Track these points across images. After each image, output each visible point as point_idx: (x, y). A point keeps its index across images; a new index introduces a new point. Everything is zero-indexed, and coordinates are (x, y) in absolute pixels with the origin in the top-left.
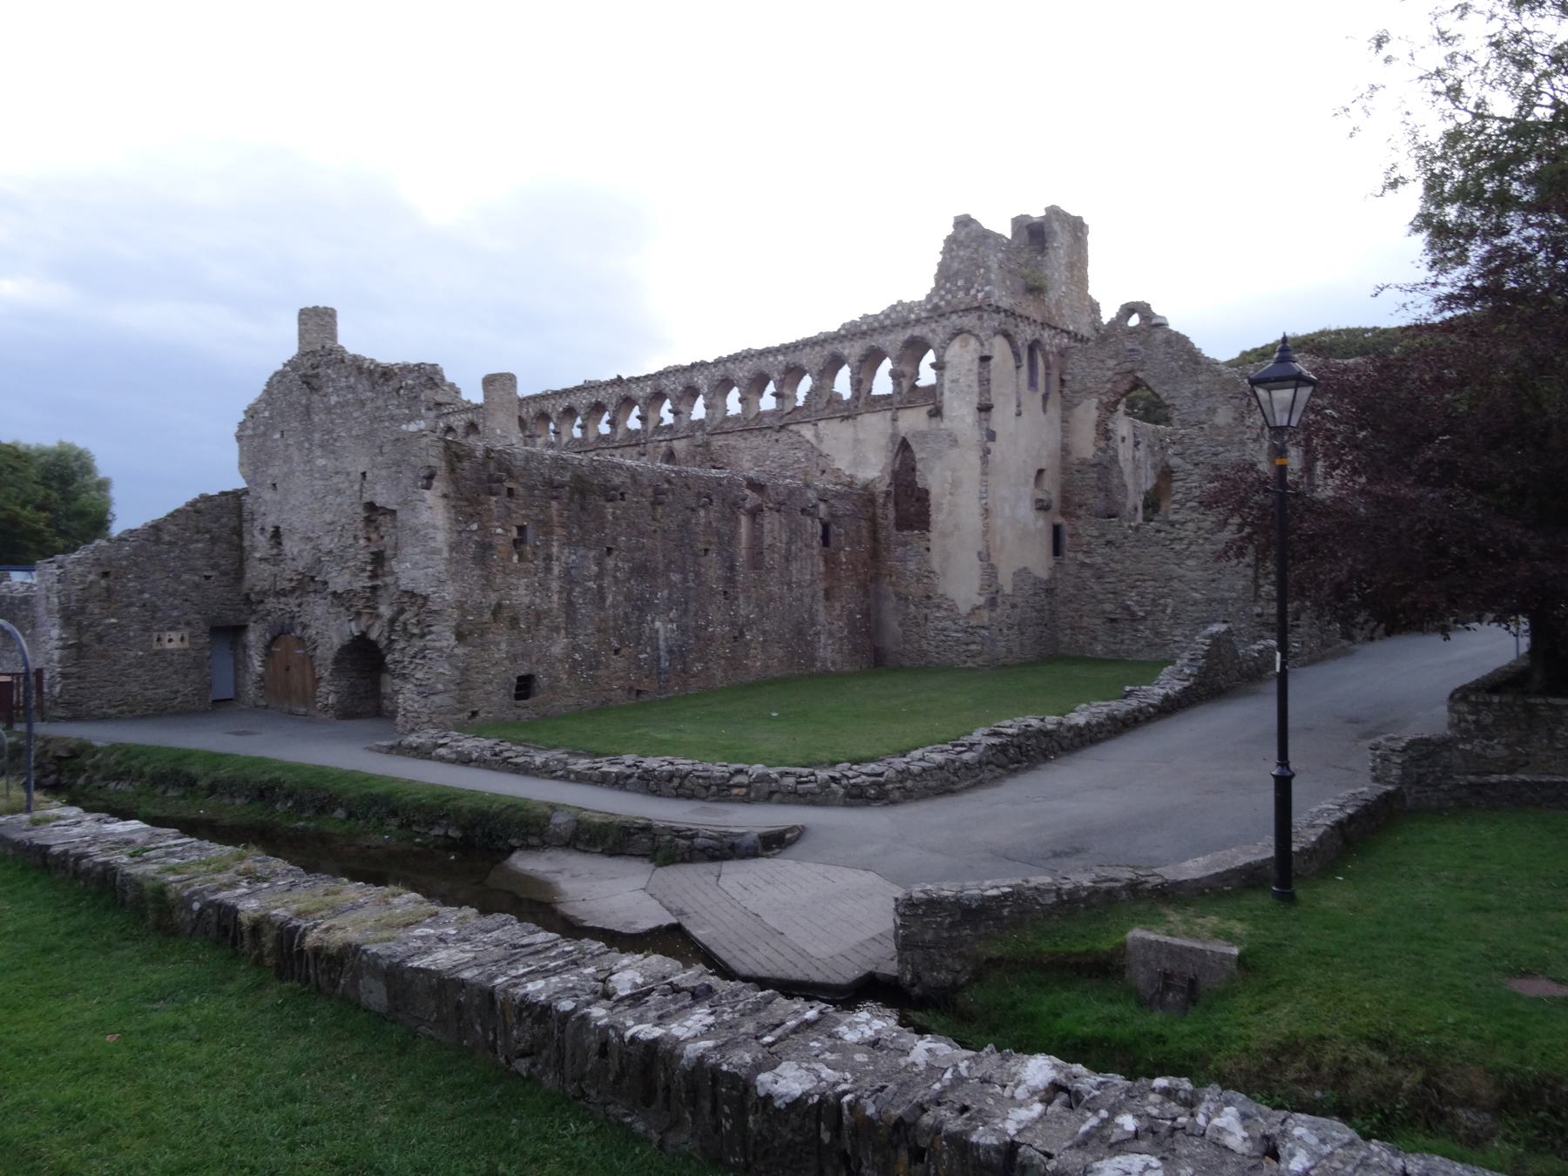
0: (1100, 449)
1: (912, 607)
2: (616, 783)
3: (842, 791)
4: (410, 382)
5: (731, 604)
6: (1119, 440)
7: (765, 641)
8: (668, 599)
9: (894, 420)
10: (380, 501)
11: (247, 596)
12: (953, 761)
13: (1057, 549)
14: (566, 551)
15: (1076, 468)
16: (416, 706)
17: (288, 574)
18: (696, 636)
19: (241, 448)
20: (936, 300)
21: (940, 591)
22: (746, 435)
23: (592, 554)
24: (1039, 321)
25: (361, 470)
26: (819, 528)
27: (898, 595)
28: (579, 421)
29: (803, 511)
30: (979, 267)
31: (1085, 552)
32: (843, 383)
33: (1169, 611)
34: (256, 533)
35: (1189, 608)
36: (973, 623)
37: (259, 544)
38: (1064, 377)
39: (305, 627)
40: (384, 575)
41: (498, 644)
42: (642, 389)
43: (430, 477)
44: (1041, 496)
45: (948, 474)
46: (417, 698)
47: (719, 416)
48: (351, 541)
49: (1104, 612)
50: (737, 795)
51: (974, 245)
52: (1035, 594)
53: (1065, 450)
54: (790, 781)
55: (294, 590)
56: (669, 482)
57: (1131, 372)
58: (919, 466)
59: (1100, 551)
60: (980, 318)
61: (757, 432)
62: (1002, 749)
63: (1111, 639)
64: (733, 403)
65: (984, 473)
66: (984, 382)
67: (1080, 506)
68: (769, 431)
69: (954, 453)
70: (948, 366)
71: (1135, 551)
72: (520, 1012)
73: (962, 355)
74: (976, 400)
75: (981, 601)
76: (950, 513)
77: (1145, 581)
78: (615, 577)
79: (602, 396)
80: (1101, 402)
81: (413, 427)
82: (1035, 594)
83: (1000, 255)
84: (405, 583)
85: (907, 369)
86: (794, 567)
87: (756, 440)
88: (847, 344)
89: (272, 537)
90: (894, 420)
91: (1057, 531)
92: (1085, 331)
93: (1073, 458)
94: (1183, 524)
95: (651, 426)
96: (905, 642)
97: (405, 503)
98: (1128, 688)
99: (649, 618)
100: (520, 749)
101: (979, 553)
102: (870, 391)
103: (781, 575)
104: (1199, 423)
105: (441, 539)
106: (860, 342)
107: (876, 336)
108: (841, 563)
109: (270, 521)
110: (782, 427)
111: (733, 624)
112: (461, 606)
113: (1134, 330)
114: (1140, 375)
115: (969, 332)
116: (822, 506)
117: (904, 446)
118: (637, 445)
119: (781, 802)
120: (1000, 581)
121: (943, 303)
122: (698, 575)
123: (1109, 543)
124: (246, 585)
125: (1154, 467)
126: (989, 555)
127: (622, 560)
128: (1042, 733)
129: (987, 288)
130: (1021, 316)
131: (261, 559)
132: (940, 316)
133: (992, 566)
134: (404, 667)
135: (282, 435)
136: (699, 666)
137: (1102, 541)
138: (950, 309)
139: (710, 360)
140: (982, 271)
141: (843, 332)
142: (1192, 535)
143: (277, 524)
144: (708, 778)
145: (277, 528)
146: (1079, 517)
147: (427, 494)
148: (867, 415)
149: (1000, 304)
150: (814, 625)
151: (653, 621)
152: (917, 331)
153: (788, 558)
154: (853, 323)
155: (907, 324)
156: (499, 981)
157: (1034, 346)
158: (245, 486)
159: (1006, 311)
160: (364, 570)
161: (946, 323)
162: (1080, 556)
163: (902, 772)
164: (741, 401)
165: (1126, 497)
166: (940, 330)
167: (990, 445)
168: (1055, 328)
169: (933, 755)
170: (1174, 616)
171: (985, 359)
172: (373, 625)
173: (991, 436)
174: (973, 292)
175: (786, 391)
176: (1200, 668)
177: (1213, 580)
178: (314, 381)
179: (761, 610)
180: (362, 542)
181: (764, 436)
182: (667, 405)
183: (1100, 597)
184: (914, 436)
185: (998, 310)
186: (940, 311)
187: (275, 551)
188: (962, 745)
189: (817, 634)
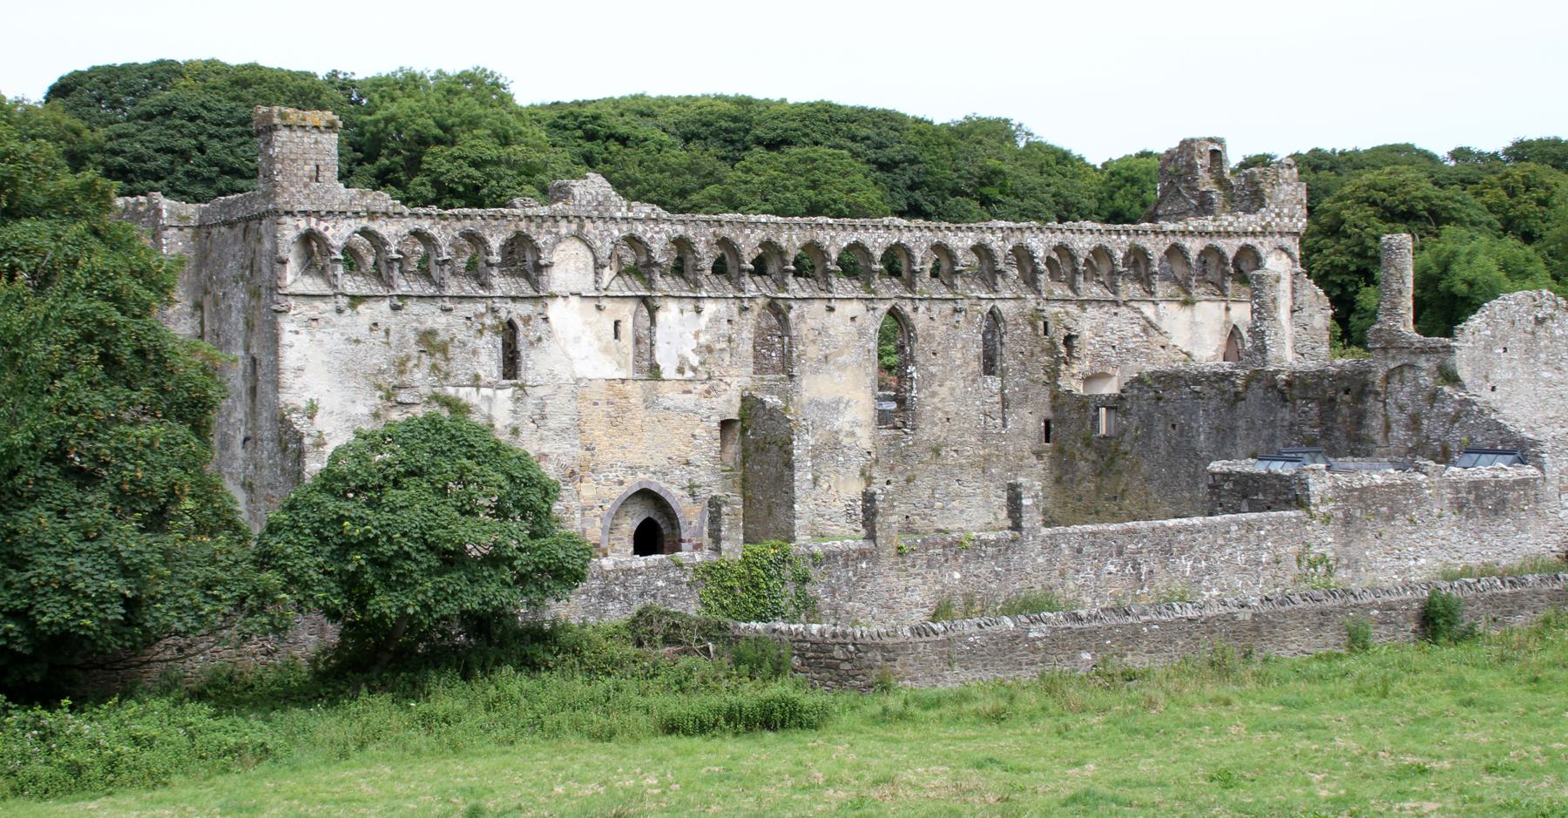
9: (1228, 309)
42: (961, 240)
51: (1295, 184)
61: (1095, 304)
90: (1228, 309)
138: (1277, 230)
152: (1250, 241)
155: (1246, 234)
166: (1266, 243)
174: (1295, 220)
186: (1269, 229)
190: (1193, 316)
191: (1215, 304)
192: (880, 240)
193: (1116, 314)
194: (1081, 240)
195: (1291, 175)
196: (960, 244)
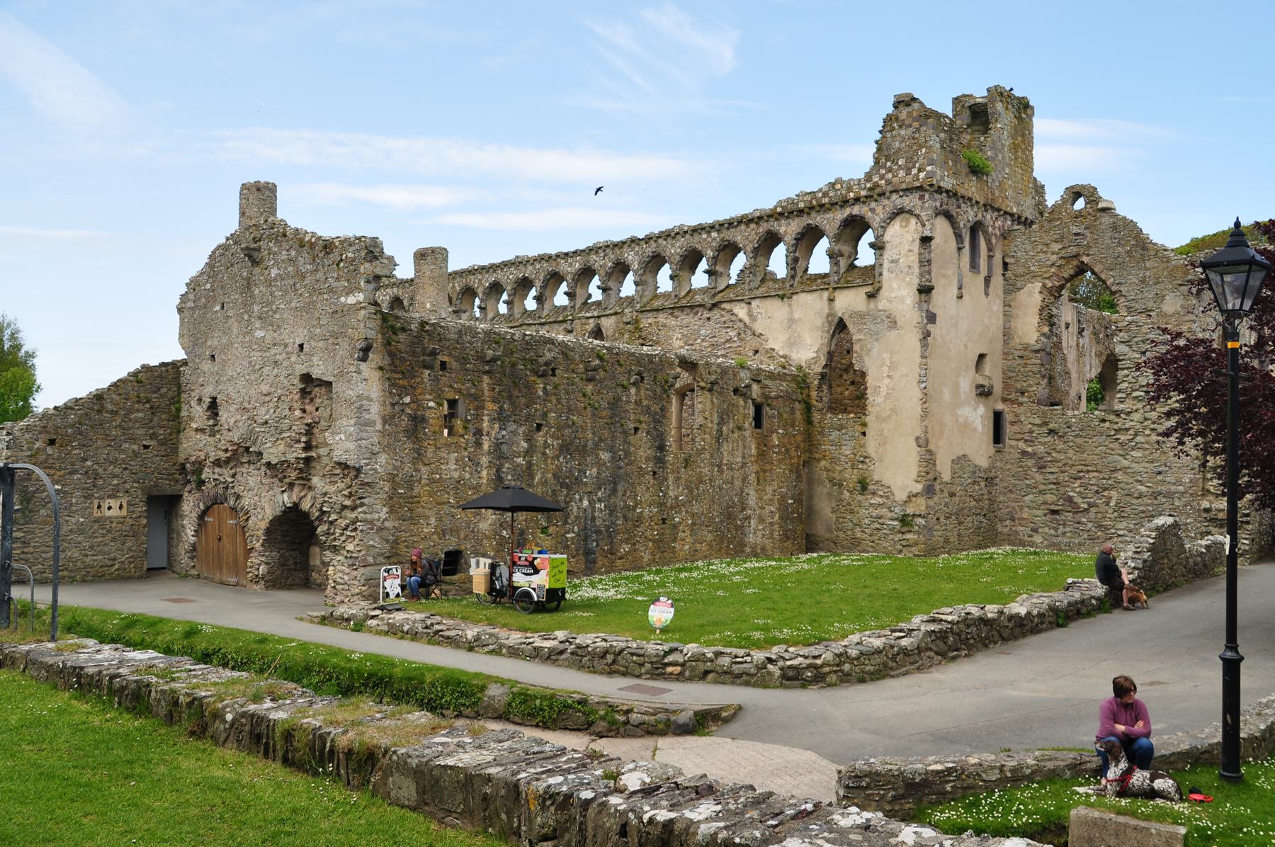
0: (1044, 335)
1: (845, 492)
2: (549, 657)
3: (778, 673)
4: (350, 255)
5: (661, 484)
6: (1063, 326)
7: (694, 524)
8: (597, 478)
9: (831, 300)
10: (316, 373)
11: (183, 466)
12: (892, 647)
13: (998, 437)
14: (497, 426)
15: (1021, 353)
16: (346, 578)
17: (222, 445)
18: (624, 517)
19: (182, 320)
20: (876, 179)
21: (876, 478)
22: (676, 313)
23: (521, 430)
24: (982, 202)
25: (298, 342)
26: (751, 411)
27: (831, 480)
28: (505, 297)
29: (736, 391)
30: (921, 147)
31: (1026, 441)
32: (778, 262)
33: (1113, 503)
34: (193, 403)
35: (1134, 501)
36: (910, 511)
37: (196, 414)
38: (1007, 260)
39: (238, 497)
40: (317, 447)
41: (427, 518)
42: (571, 265)
43: (366, 350)
44: (981, 381)
45: (886, 356)
46: (348, 570)
47: (648, 294)
48: (287, 412)
49: (1045, 503)
50: (671, 674)
51: (916, 124)
52: (974, 483)
53: (1007, 334)
54: (725, 661)
55: (228, 460)
56: (600, 357)
57: (1077, 256)
58: (856, 348)
59: (1043, 440)
60: (921, 198)
62: (941, 636)
63: (1052, 532)
64: (664, 280)
65: (923, 357)
66: (925, 263)
67: (1023, 393)
68: (701, 309)
69: (892, 335)
70: (888, 246)
71: (1079, 440)
72: (544, 801)
73: (902, 236)
74: (916, 282)
75: (918, 488)
76: (888, 396)
77: (1088, 471)
78: (544, 454)
79: (529, 271)
80: (1044, 286)
81: (351, 300)
82: (974, 483)
83: (942, 135)
84: (338, 455)
85: (846, 249)
86: (726, 448)
87: (686, 318)
88: (783, 222)
89: (209, 408)
90: (831, 300)
91: (998, 417)
92: (1029, 214)
93: (1016, 342)
94: (1129, 413)
95: (579, 303)
96: (838, 529)
97: (341, 374)
98: (1070, 580)
99: (577, 496)
100: (451, 622)
101: (917, 439)
102: (807, 269)
103: (712, 456)
104: (1147, 312)
105: (375, 411)
106: (797, 220)
107: (813, 214)
108: (774, 446)
109: (208, 391)
110: (715, 305)
111: (661, 505)
112: (392, 478)
113: (1079, 215)
114: (1085, 259)
115: (910, 212)
116: (755, 387)
117: (841, 326)
118: (564, 321)
119: (716, 682)
120: (938, 468)
121: (883, 182)
122: (627, 454)
123: (1051, 432)
124: (182, 456)
125: (1099, 354)
126: (927, 441)
127: (552, 437)
128: (983, 621)
129: (929, 168)
130: (963, 197)
131: (197, 430)
132: (880, 195)
133: (929, 452)
134: (335, 539)
135: (223, 307)
136: (627, 548)
137: (1045, 429)
138: (889, 188)
139: (641, 236)
140: (924, 150)
141: (779, 210)
142: (1138, 426)
143: (214, 394)
144: (643, 655)
145: (214, 399)
146: (1021, 404)
147: (363, 366)
148: (803, 295)
149: (942, 184)
150: (744, 509)
151: (581, 500)
152: (856, 210)
153: (719, 438)
154: (791, 201)
155: (845, 203)
156: (523, 775)
157: (976, 228)
158: (186, 357)
159: (947, 192)
160: (298, 441)
161: (886, 202)
162: (1021, 445)
163: (839, 655)
164: (672, 278)
165: (1070, 385)
166: (879, 209)
167: (930, 327)
168: (999, 210)
169: (871, 640)
170: (1119, 509)
171: (926, 240)
172: (305, 496)
173: (932, 318)
174: (914, 171)
175: (719, 268)
176: (1145, 561)
177: (1160, 473)
178: (255, 254)
179: (691, 491)
180: (298, 413)
181: (696, 313)
182: (596, 281)
183: (1042, 487)
184: (851, 316)
185: (939, 190)
186: (878, 190)
187: (211, 422)
188: (901, 631)
189: (748, 518)
190: (791, 312)
191: (815, 295)
192: (511, 277)
193: (709, 319)
194: (673, 245)
195: (909, 114)
196: (569, 269)
